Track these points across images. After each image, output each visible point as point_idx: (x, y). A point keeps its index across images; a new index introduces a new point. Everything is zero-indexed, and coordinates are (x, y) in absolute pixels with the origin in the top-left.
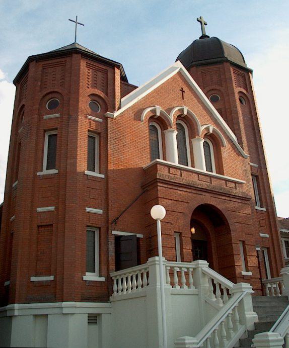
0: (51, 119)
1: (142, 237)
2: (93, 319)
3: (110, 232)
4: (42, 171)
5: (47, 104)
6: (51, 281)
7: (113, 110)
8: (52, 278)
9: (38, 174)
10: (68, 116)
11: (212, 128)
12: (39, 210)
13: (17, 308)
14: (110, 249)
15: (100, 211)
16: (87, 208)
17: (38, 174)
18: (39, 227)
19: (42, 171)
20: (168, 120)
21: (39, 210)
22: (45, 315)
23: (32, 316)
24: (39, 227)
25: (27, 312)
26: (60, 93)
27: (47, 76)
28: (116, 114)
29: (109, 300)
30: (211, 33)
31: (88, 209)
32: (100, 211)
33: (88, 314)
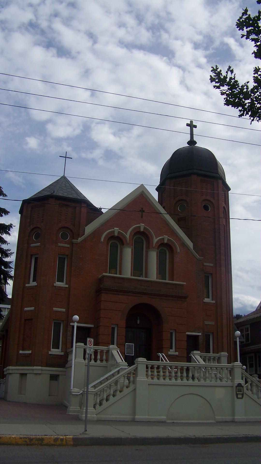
0: (35, 247)
1: (93, 326)
2: (54, 378)
3: (69, 324)
4: (29, 283)
5: (61, 233)
6: (30, 354)
7: (79, 236)
8: (30, 352)
9: (26, 286)
10: (74, 241)
11: (166, 238)
12: (26, 309)
13: (10, 368)
14: (68, 335)
15: (64, 310)
16: (54, 309)
17: (26, 286)
18: (26, 320)
19: (29, 283)
20: (125, 237)
21: (26, 309)
22: (25, 373)
23: (19, 374)
24: (26, 320)
25: (16, 371)
26: (40, 228)
27: (38, 216)
28: (80, 239)
29: (65, 366)
30: (201, 144)
31: (55, 309)
32: (64, 310)
33: (50, 374)
